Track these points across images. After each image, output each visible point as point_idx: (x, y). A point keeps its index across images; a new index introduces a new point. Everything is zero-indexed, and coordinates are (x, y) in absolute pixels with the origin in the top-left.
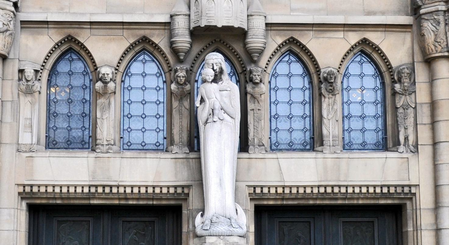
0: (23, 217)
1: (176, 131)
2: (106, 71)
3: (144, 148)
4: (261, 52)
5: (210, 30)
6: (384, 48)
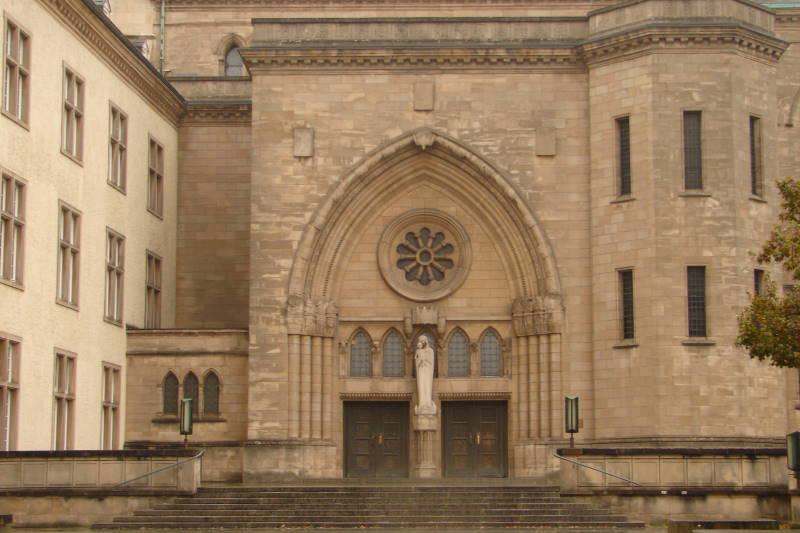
0: (342, 407)
1: (407, 368)
2: (376, 343)
3: (393, 376)
4: (444, 334)
6: (499, 330)
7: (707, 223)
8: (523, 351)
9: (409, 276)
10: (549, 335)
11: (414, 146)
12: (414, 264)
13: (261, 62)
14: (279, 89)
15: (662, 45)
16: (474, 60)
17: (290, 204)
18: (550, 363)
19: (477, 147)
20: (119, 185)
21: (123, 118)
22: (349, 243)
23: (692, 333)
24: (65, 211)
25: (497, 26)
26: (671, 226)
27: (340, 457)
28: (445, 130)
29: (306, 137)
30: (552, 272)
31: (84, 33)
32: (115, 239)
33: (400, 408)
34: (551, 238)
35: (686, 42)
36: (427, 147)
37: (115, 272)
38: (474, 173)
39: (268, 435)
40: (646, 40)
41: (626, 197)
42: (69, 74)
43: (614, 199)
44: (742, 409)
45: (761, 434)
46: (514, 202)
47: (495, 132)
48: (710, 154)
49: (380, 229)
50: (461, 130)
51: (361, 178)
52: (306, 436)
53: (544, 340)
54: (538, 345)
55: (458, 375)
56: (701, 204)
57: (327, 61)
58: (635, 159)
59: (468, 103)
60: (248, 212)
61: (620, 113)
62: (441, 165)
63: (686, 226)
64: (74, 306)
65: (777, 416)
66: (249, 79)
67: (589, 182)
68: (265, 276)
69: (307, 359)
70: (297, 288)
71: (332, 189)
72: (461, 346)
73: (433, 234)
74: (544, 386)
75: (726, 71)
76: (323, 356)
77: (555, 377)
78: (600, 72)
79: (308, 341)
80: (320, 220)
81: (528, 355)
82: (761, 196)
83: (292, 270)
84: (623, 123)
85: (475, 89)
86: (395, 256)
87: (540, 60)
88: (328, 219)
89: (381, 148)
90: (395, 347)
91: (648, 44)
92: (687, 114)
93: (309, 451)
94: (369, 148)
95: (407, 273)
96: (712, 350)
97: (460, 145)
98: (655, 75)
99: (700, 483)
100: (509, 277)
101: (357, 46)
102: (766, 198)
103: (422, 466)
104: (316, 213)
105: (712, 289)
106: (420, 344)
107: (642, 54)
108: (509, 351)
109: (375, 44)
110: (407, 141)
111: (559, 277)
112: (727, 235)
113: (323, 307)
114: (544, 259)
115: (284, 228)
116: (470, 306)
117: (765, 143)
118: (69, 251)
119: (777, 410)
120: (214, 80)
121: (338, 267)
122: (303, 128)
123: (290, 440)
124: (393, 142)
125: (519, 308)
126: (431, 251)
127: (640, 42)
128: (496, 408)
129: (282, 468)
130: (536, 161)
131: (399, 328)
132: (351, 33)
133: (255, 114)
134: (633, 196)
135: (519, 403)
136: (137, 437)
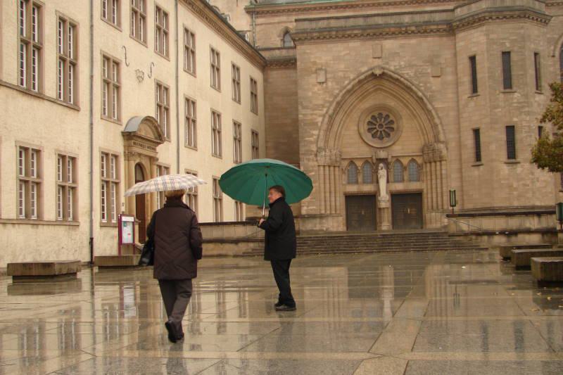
2: (359, 168)
3: (368, 183)
5: (380, 159)
7: (515, 105)
8: (428, 169)
9: (374, 136)
10: (440, 161)
11: (373, 75)
12: (375, 130)
13: (300, 39)
14: (308, 51)
15: (490, 20)
16: (400, 33)
17: (316, 105)
18: (441, 174)
19: (403, 74)
20: (237, 100)
21: (238, 69)
22: (344, 122)
23: (509, 158)
24: (214, 113)
25: (410, 16)
26: (498, 107)
27: (345, 222)
28: (387, 66)
29: (323, 73)
30: (441, 131)
31: (219, 31)
32: (237, 125)
33: (372, 198)
34: (440, 115)
35: (502, 19)
36: (380, 75)
37: (238, 140)
38: (403, 86)
39: (313, 212)
40: (482, 19)
41: (475, 95)
42: (213, 50)
43: (469, 95)
44: (534, 193)
45: (543, 204)
46: (421, 99)
47: (411, 66)
48: (515, 72)
49: (359, 114)
50: (395, 66)
51: (348, 91)
52: (328, 212)
53: (438, 163)
54: (436, 166)
55: (398, 182)
56: (512, 96)
57: (331, 37)
58: (479, 76)
59: (397, 53)
60: (297, 110)
61: (471, 54)
62: (387, 84)
63: (505, 107)
64: (220, 156)
65: (551, 195)
66: (295, 47)
67: (457, 88)
68: (307, 139)
69: (327, 177)
70: (321, 144)
71: (336, 97)
72: (399, 168)
73: (384, 116)
74: (439, 186)
75: (522, 31)
76: (334, 175)
77: (444, 181)
78: (460, 35)
79: (327, 168)
80: (331, 112)
81: (431, 171)
82: (540, 90)
83: (319, 135)
84: (473, 59)
85: (402, 46)
86: (366, 127)
87: (432, 31)
88: (334, 111)
89: (358, 77)
90: (368, 169)
91: (483, 20)
92: (504, 53)
93: (330, 219)
94: (352, 76)
95: (373, 135)
96: (519, 165)
97: (395, 73)
98: (487, 35)
99: (514, 228)
100: (421, 135)
101: (344, 29)
102: (543, 92)
103: (383, 224)
104: (329, 108)
105: (518, 136)
106: (380, 168)
107: (480, 25)
108: (422, 169)
109: (353, 28)
110: (370, 72)
111: (444, 133)
112: (524, 110)
113: (334, 152)
114: (437, 125)
115: (314, 116)
116: (403, 149)
117: (542, 65)
118: (216, 131)
119: (551, 193)
120: (279, 49)
121: (340, 133)
122: (321, 69)
123: (321, 214)
124: (363, 73)
125: (426, 149)
126: (384, 124)
127: (480, 20)
128: (417, 196)
129: (318, 227)
130: (432, 79)
131: (370, 160)
132: (342, 23)
133: (298, 63)
134: (478, 94)
135: (427, 194)
136: (251, 215)
